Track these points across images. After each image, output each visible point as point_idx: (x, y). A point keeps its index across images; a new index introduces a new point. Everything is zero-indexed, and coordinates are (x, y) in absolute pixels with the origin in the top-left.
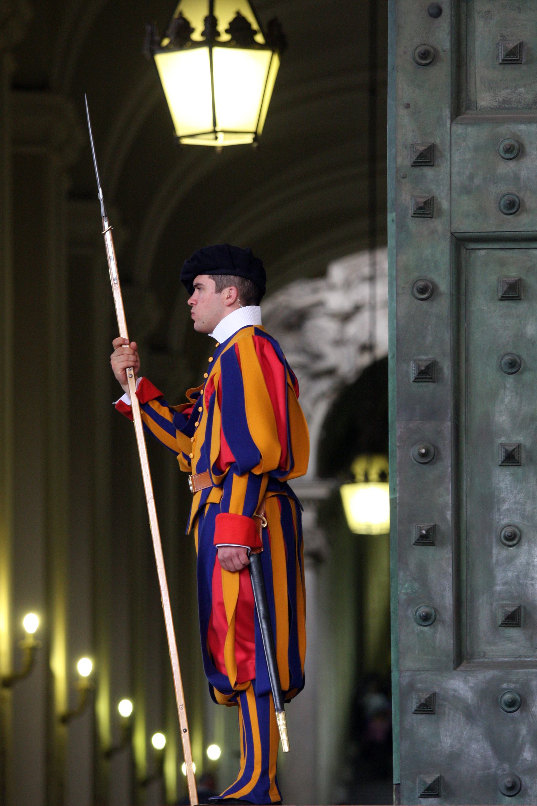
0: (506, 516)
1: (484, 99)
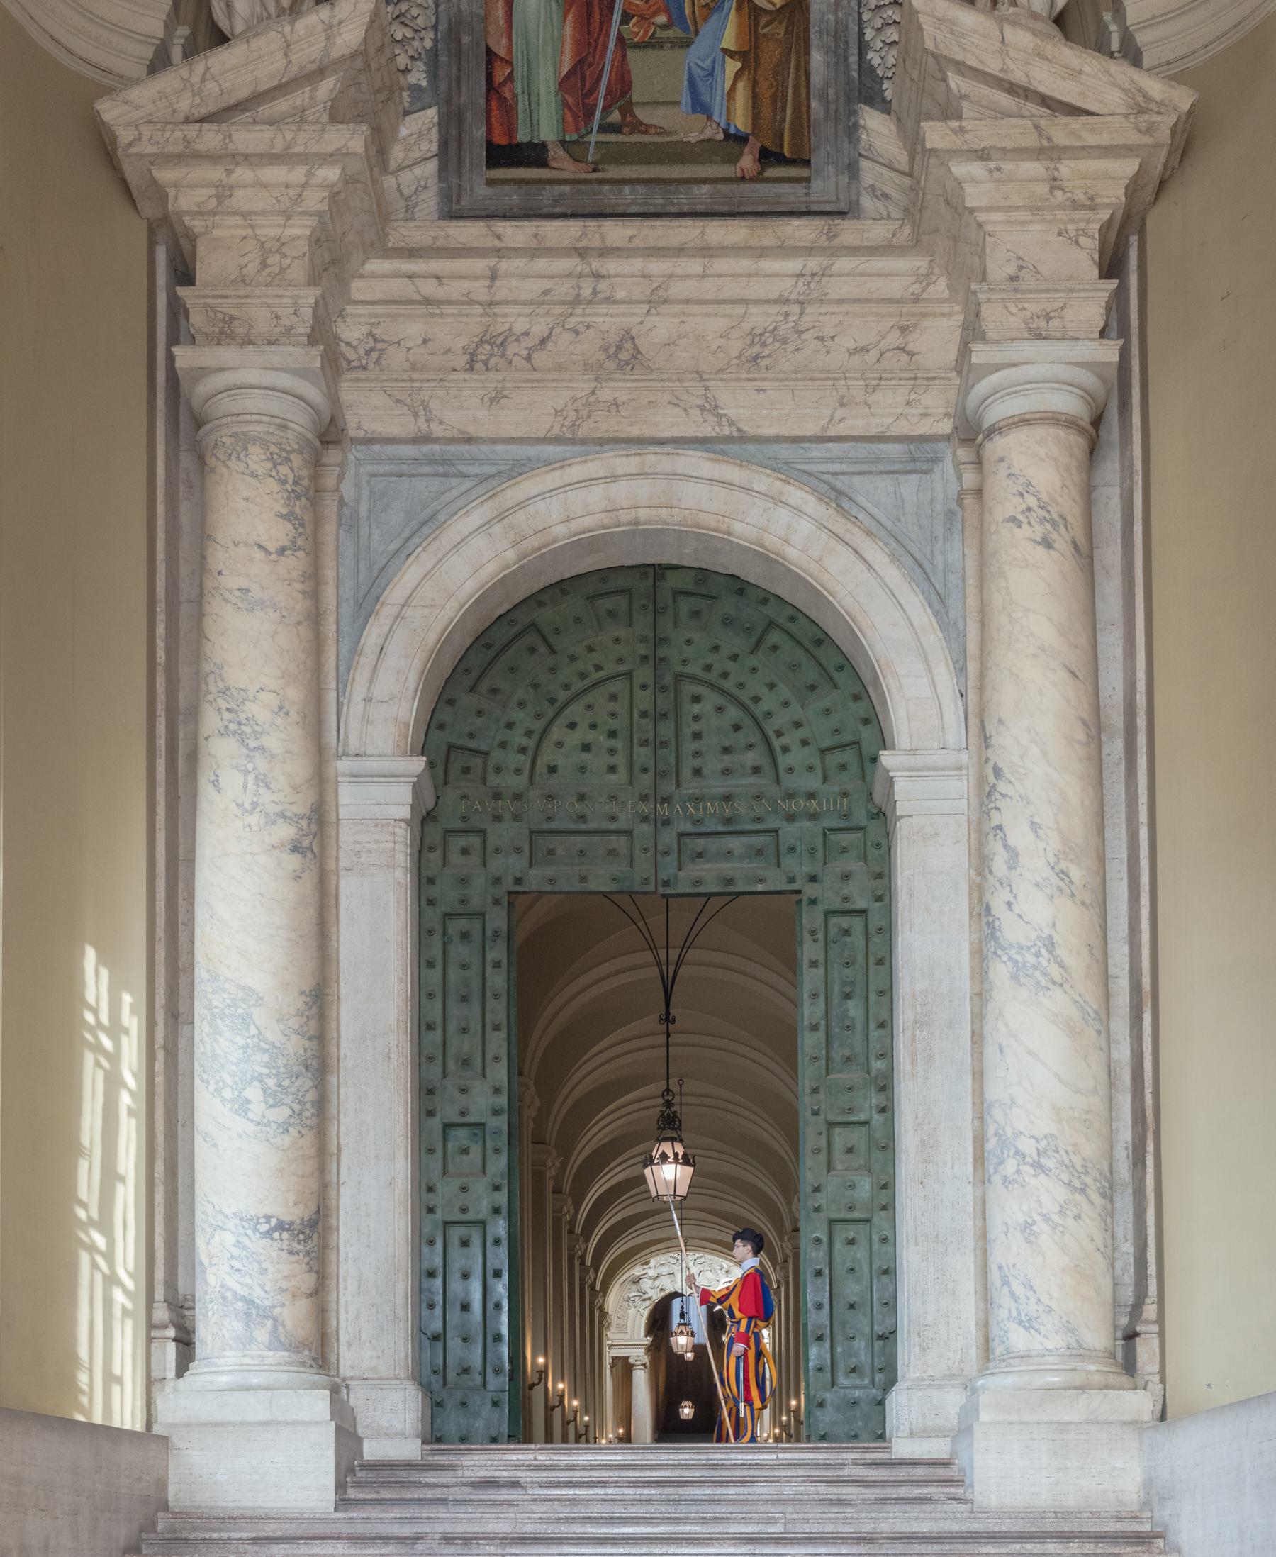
1: (839, 1167)
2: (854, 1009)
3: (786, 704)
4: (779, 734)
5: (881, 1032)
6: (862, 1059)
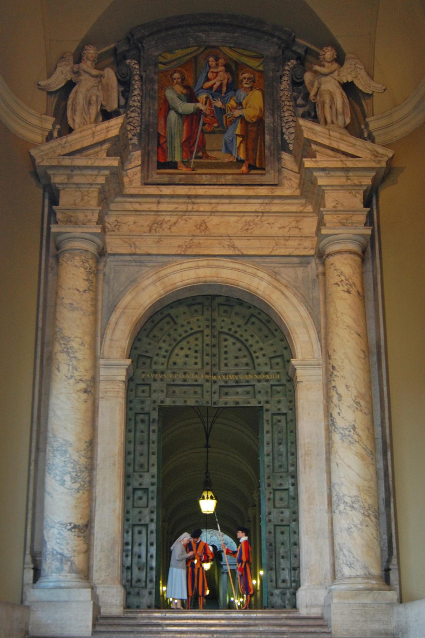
0: (282, 566)
2: (282, 448)
3: (257, 342)
4: (255, 352)
5: (293, 457)
6: (286, 466)
